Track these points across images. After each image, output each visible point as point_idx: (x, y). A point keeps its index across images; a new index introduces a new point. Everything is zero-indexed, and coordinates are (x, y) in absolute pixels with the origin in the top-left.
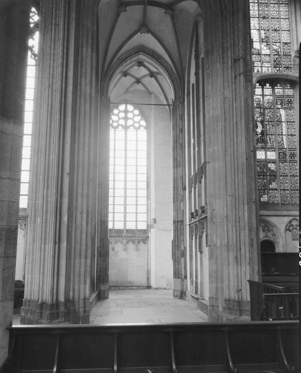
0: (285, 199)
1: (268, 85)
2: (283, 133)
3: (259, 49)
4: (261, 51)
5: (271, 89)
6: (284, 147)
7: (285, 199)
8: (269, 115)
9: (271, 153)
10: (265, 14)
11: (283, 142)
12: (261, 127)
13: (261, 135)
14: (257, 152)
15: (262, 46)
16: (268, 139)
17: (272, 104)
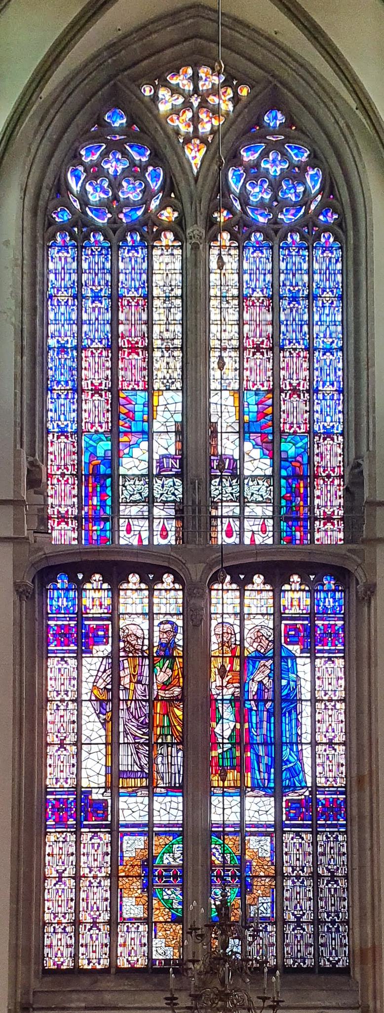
0: (299, 951)
1: (258, 579)
2: (304, 736)
3: (236, 457)
4: (242, 468)
5: (271, 594)
6: (303, 784)
7: (299, 951)
8: (258, 678)
9: (261, 804)
10: (261, 336)
11: (302, 764)
12: (232, 718)
13: (230, 746)
14: (213, 798)
15: (248, 446)
16: (253, 757)
17: (270, 641)
